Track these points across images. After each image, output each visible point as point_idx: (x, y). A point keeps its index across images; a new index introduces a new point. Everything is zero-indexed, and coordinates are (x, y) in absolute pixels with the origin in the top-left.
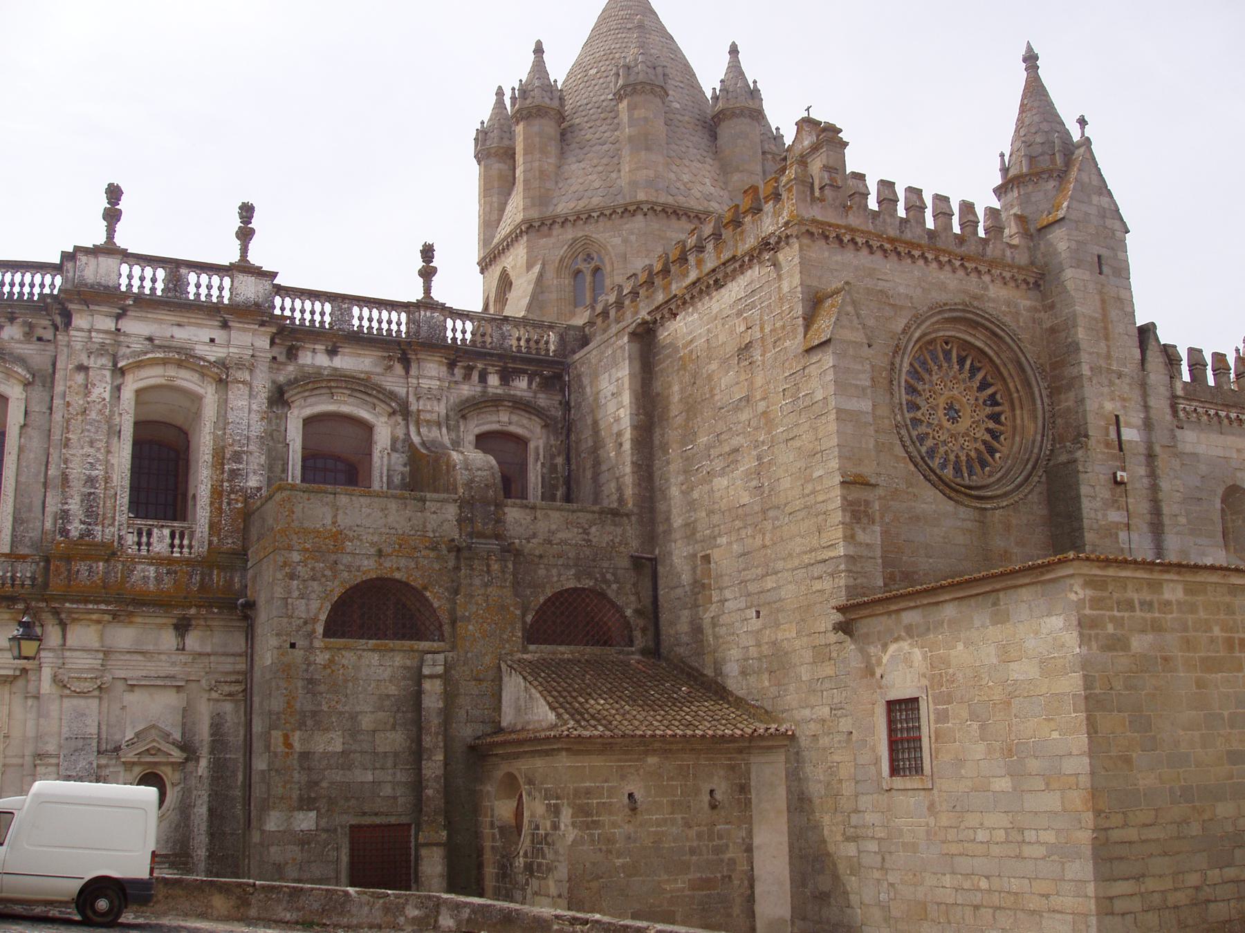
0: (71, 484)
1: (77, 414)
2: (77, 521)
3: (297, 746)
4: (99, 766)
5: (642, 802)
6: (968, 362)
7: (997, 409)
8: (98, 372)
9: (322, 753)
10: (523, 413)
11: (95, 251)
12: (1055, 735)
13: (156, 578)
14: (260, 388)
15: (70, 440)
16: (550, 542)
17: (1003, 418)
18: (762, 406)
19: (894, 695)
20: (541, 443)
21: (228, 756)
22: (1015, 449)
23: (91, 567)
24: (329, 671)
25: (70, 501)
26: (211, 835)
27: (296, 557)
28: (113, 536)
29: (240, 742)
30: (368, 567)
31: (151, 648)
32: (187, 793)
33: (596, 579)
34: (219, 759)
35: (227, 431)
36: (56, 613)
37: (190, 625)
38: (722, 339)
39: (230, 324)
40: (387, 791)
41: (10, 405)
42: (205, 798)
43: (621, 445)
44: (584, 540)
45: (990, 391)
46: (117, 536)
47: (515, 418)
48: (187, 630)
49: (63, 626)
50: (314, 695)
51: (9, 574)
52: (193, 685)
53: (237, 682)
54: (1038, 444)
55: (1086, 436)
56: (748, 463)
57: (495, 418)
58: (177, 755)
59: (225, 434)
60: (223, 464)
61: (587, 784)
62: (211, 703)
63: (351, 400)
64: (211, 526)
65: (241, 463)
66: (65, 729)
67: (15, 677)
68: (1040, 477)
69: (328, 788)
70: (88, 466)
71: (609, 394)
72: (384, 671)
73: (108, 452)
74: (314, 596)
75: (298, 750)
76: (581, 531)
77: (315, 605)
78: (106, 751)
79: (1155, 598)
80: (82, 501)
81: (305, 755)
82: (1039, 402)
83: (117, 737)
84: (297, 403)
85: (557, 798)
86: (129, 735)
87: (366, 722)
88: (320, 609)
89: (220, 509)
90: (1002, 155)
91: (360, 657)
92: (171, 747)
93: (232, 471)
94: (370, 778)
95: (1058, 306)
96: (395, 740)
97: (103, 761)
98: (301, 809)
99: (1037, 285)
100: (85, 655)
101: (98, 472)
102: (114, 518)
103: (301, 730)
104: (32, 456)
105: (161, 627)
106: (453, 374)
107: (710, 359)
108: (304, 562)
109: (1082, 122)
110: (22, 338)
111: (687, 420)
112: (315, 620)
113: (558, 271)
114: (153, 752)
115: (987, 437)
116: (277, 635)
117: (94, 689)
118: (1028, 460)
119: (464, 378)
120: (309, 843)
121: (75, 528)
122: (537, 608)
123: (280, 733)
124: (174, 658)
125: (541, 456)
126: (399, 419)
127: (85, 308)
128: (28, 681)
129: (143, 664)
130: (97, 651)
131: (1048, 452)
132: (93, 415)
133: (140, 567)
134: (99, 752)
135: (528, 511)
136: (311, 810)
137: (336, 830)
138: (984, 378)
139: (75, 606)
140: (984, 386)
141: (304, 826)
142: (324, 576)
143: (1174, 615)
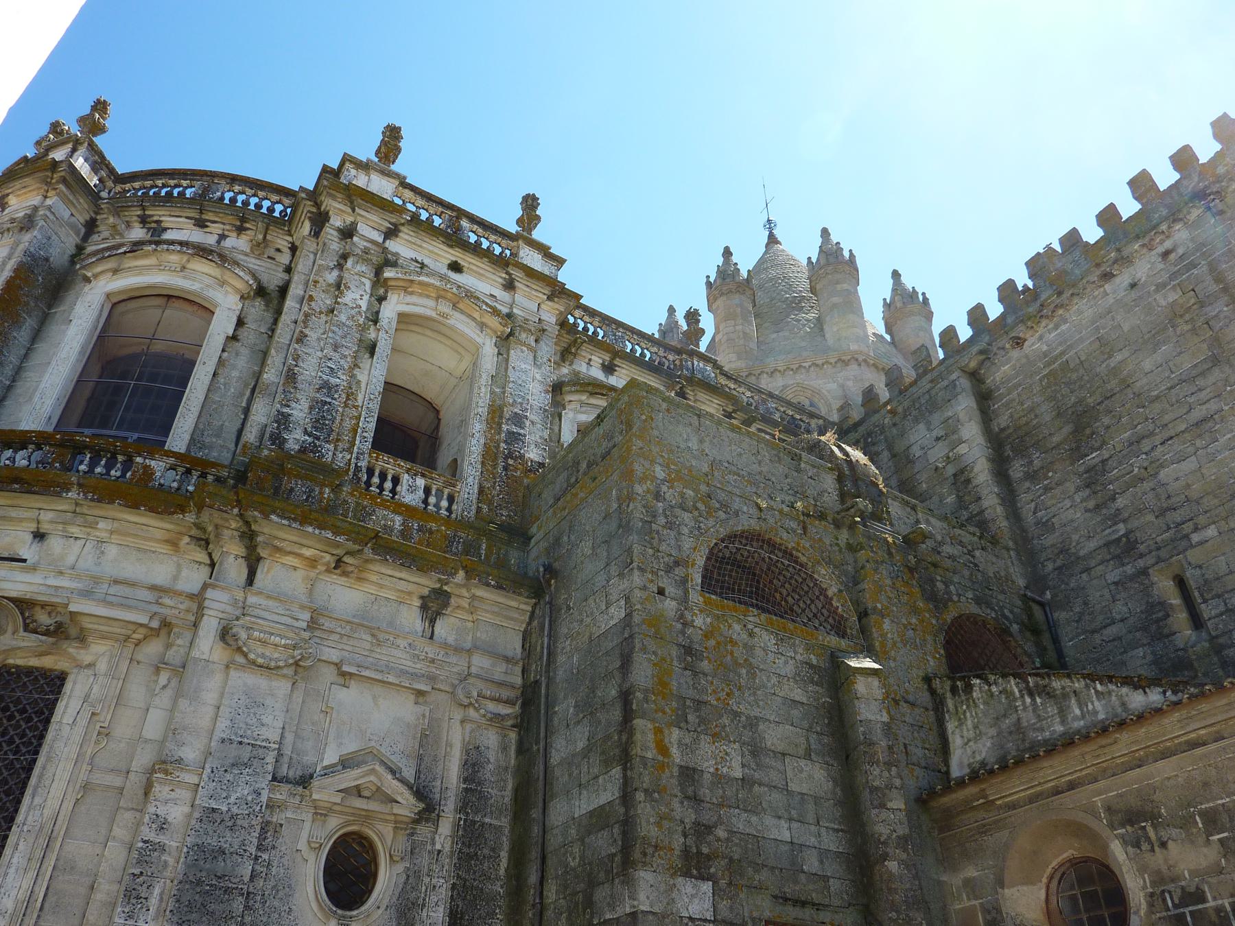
1: (321, 313)
4: (271, 805)
9: (712, 774)
14: (545, 360)
21: (487, 820)
23: (313, 490)
25: (293, 405)
27: (660, 473)
29: (507, 800)
32: (412, 878)
34: (474, 822)
39: (517, 284)
40: (811, 864)
42: (444, 892)
46: (353, 465)
50: (695, 674)
58: (407, 804)
59: (504, 393)
60: (500, 424)
64: (481, 490)
66: (223, 724)
69: (728, 840)
70: (327, 371)
72: (786, 663)
74: (685, 530)
80: (311, 408)
83: (309, 759)
84: (572, 406)
86: (331, 757)
93: (510, 433)
94: (786, 836)
101: (340, 380)
104: (235, 374)
110: (248, 251)
121: (295, 439)
133: (381, 512)
134: (274, 779)
136: (703, 878)
142: (697, 509)
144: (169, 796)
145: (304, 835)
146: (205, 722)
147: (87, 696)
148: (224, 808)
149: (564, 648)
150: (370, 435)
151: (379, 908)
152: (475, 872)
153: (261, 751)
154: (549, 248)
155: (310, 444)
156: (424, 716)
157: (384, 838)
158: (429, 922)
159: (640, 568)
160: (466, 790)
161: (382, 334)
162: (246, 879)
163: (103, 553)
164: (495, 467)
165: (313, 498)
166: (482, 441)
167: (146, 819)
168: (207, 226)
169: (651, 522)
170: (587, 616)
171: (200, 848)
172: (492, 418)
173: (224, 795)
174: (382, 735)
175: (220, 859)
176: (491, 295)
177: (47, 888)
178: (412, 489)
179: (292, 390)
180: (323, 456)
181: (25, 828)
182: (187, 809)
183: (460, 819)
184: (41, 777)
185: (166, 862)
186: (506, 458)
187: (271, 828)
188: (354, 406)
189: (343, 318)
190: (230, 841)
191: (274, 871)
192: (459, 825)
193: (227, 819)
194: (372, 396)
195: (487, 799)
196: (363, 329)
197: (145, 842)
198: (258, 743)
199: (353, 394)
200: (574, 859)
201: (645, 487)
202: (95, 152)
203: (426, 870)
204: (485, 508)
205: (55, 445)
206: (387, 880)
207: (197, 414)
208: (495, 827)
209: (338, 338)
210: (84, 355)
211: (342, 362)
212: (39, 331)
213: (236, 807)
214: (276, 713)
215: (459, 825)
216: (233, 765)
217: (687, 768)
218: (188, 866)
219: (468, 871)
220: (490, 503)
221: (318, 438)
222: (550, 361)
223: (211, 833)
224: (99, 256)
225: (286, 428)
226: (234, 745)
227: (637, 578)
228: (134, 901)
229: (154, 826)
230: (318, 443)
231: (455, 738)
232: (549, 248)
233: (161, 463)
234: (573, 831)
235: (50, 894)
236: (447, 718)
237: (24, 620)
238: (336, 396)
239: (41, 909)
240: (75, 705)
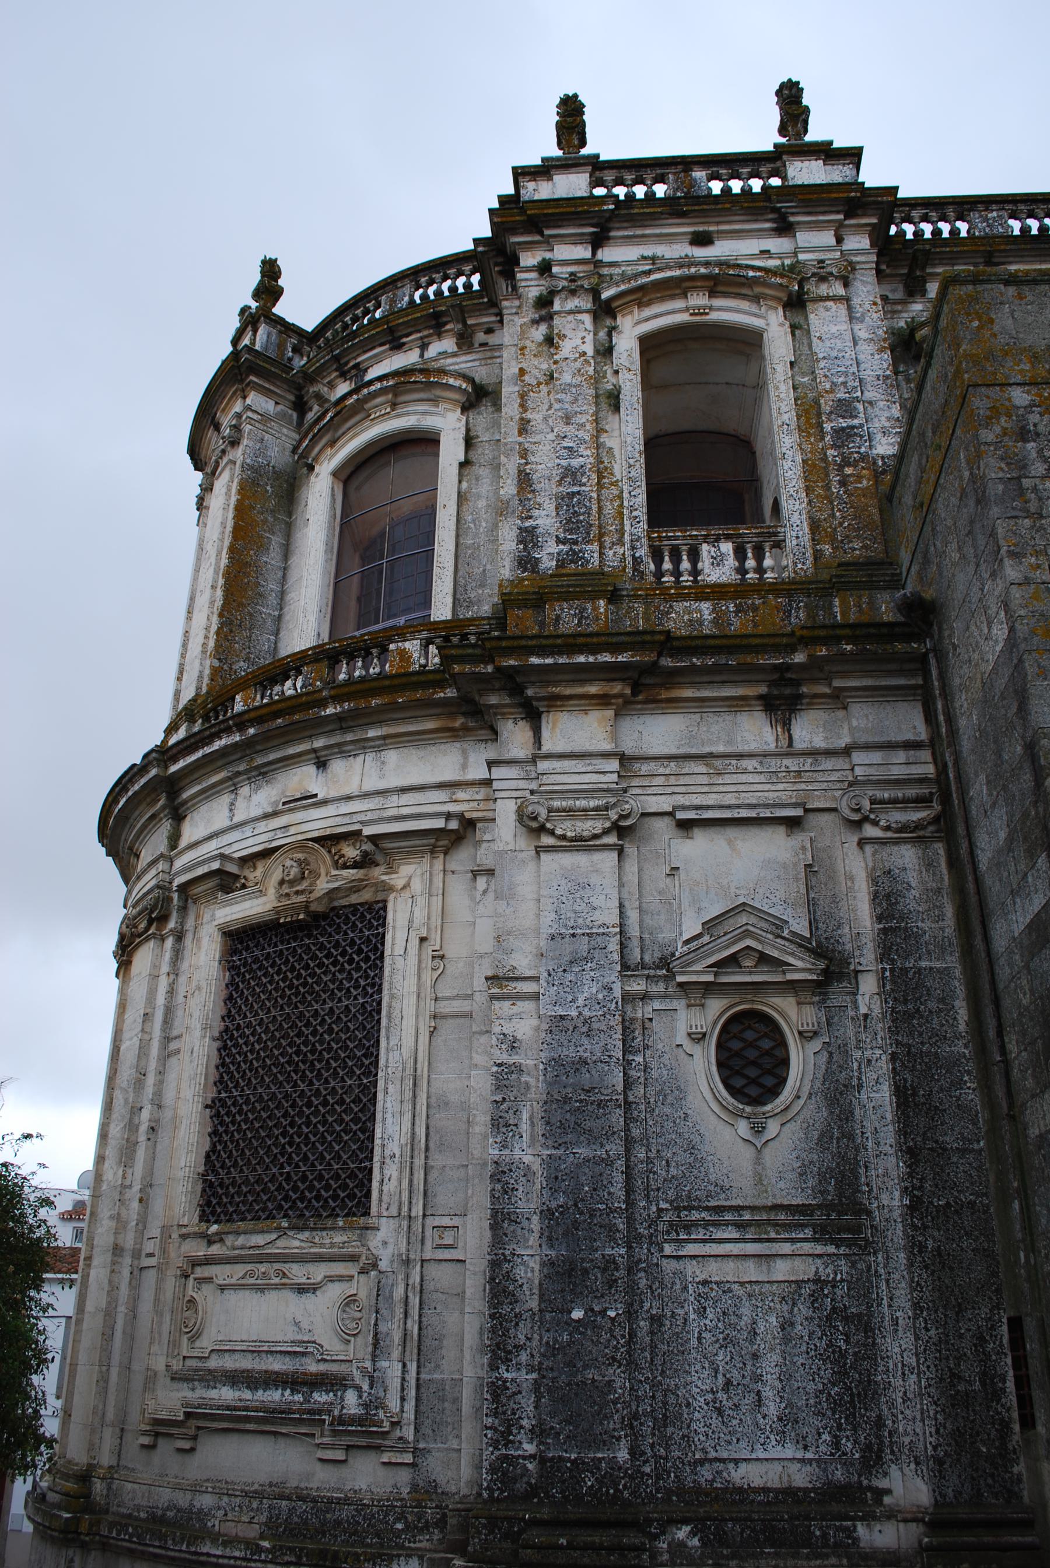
0: (537, 487)
1: (539, 384)
2: (552, 543)
8: (570, 318)
11: (545, 170)
14: (867, 306)
15: (529, 421)
21: (924, 964)
23: (585, 609)
25: (536, 513)
26: (911, 1154)
31: (721, 749)
34: (905, 971)
35: (819, 373)
42: (884, 1065)
49: (533, 717)
52: (825, 819)
60: (820, 425)
62: (869, 849)
64: (815, 526)
65: (856, 417)
70: (564, 452)
73: (600, 431)
78: (643, 965)
83: (665, 936)
86: (691, 927)
93: (838, 432)
97: (637, 986)
102: (621, 532)
105: (737, 704)
110: (456, 349)
117: (606, 832)
124: (774, 764)
127: (538, 238)
129: (704, 780)
130: (605, 755)
132: (567, 378)
133: (679, 606)
134: (625, 966)
139: (549, 661)
144: (511, 1012)
147: (411, 921)
148: (574, 1014)
149: (962, 706)
150: (642, 513)
151: (799, 1097)
152: (921, 1034)
153: (599, 939)
154: (831, 143)
155: (567, 553)
156: (803, 848)
158: (872, 1104)
159: (1012, 554)
160: (884, 931)
161: (624, 376)
162: (620, 1088)
163: (383, 763)
164: (827, 487)
165: (588, 618)
166: (799, 459)
167: (494, 1041)
168: (404, 344)
169: (1019, 478)
170: (974, 651)
172: (808, 421)
173: (570, 998)
174: (751, 885)
175: (584, 1070)
176: (762, 252)
177: (427, 1128)
178: (718, 561)
179: (530, 496)
180: (588, 562)
181: (390, 1071)
183: (884, 970)
184: (389, 1017)
185: (527, 1083)
186: (841, 468)
187: (638, 1025)
188: (612, 484)
189: (567, 378)
190: (589, 1049)
191: (655, 1074)
192: (884, 978)
193: (580, 1025)
194: (632, 461)
195: (918, 936)
196: (597, 379)
197: (499, 1065)
198: (594, 930)
199: (606, 468)
200: (1025, 994)
201: (998, 429)
202: (275, 321)
203: (853, 1042)
204: (827, 549)
205: (311, 662)
207: (452, 569)
208: (938, 970)
209: (567, 406)
210: (332, 551)
211: (581, 434)
212: (288, 545)
213: (586, 1009)
214: (607, 891)
215: (884, 978)
216: (571, 962)
218: (550, 1084)
219: (911, 1034)
220: (833, 539)
221: (576, 542)
222: (875, 304)
223: (565, 1043)
224: (310, 436)
225: (536, 545)
226: (567, 940)
227: (1011, 571)
228: (504, 1130)
229: (503, 1047)
230: (576, 548)
232: (831, 143)
233: (415, 642)
234: (1017, 957)
235: (431, 1134)
236: (838, 844)
237: (333, 857)
238: (584, 480)
239: (427, 1149)
240: (401, 936)
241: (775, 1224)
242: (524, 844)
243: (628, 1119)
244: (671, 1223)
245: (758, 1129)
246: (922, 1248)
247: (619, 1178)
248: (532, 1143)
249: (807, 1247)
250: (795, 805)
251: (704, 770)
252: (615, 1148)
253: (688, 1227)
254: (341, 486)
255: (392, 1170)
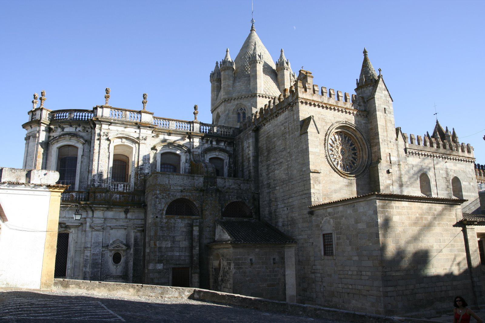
2: (97, 182)
3: (158, 245)
4: (102, 251)
5: (254, 262)
6: (347, 138)
7: (355, 151)
10: (223, 152)
12: (371, 244)
13: (119, 198)
16: (229, 188)
17: (357, 154)
18: (288, 150)
19: (325, 232)
20: (228, 161)
22: (360, 163)
24: (167, 224)
26: (134, 270)
27: (158, 192)
28: (107, 186)
30: (179, 196)
31: (117, 217)
33: (242, 199)
34: (136, 249)
36: (91, 208)
37: (129, 211)
38: (277, 131)
40: (183, 258)
41: (79, 149)
42: (132, 260)
43: (250, 161)
44: (239, 188)
45: (353, 146)
47: (220, 154)
48: (128, 212)
49: (93, 211)
51: (78, 197)
52: (130, 228)
53: (142, 227)
54: (367, 161)
55: (381, 159)
56: (285, 166)
57: (213, 154)
58: (124, 248)
61: (238, 257)
63: (174, 148)
64: (135, 183)
66: (93, 240)
67: (79, 226)
68: (367, 171)
71: (246, 147)
72: (183, 224)
74: (163, 203)
75: (158, 246)
76: (238, 185)
77: (163, 206)
78: (105, 246)
79: (400, 205)
80: (98, 177)
81: (160, 248)
82: (367, 149)
83: (108, 242)
85: (230, 260)
86: (111, 242)
87: (177, 239)
88: (165, 207)
89: (137, 179)
90: (357, 80)
91: (176, 221)
92: (123, 245)
94: (178, 254)
95: (373, 122)
96: (185, 244)
97: (104, 249)
98: (159, 263)
99: (367, 116)
100: (99, 219)
103: (159, 241)
104: (85, 164)
105: (120, 211)
106: (203, 141)
107: (274, 137)
108: (160, 194)
109: (380, 70)
111: (268, 154)
112: (163, 210)
113: (233, 113)
114: (118, 247)
115: (352, 159)
116: (153, 214)
118: (364, 166)
119: (206, 142)
120: (161, 273)
121: (96, 184)
122: (226, 207)
123: (153, 242)
124: (124, 220)
125: (227, 165)
126: (188, 154)
127: (100, 123)
128: (83, 227)
129: (115, 222)
131: (370, 164)
134: (102, 247)
135: (223, 180)
136: (161, 263)
137: (168, 269)
138: (352, 142)
139: (96, 206)
140: (351, 145)
141: (160, 268)
143: (405, 210)
145: (109, 254)
146: (90, 240)
147: (72, 237)
157: (122, 253)
164: (138, 177)
171: (93, 259)
182: (90, 254)
190: (97, 257)
206: (123, 259)
217: (160, 247)
231: (132, 235)
241: (118, 278)
242: (90, 230)
243: (101, 266)
244: (105, 278)
245: (117, 267)
246: (134, 281)
247: (100, 273)
248: (89, 268)
249: (121, 280)
250: (126, 226)
251: (115, 220)
252: (99, 269)
253: (107, 278)
254: (58, 149)
255: (69, 271)
